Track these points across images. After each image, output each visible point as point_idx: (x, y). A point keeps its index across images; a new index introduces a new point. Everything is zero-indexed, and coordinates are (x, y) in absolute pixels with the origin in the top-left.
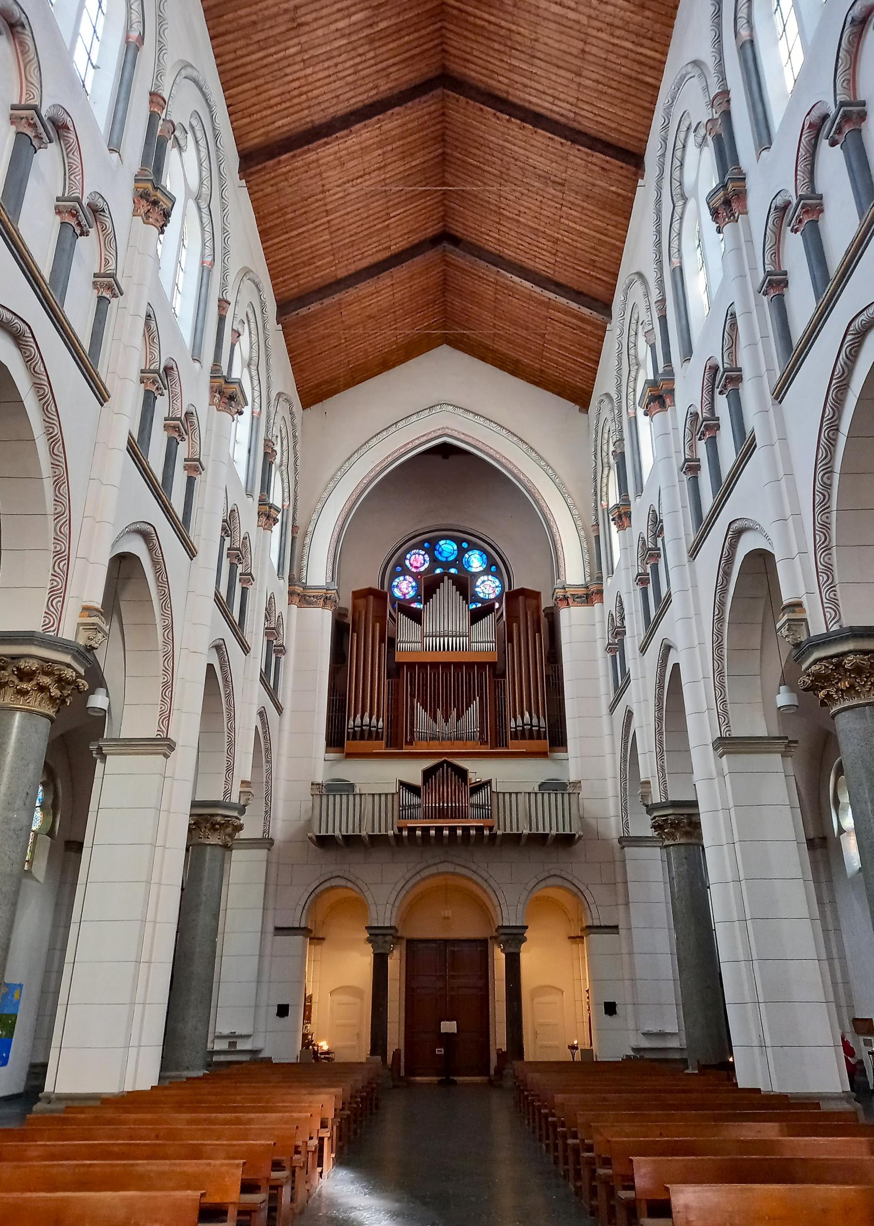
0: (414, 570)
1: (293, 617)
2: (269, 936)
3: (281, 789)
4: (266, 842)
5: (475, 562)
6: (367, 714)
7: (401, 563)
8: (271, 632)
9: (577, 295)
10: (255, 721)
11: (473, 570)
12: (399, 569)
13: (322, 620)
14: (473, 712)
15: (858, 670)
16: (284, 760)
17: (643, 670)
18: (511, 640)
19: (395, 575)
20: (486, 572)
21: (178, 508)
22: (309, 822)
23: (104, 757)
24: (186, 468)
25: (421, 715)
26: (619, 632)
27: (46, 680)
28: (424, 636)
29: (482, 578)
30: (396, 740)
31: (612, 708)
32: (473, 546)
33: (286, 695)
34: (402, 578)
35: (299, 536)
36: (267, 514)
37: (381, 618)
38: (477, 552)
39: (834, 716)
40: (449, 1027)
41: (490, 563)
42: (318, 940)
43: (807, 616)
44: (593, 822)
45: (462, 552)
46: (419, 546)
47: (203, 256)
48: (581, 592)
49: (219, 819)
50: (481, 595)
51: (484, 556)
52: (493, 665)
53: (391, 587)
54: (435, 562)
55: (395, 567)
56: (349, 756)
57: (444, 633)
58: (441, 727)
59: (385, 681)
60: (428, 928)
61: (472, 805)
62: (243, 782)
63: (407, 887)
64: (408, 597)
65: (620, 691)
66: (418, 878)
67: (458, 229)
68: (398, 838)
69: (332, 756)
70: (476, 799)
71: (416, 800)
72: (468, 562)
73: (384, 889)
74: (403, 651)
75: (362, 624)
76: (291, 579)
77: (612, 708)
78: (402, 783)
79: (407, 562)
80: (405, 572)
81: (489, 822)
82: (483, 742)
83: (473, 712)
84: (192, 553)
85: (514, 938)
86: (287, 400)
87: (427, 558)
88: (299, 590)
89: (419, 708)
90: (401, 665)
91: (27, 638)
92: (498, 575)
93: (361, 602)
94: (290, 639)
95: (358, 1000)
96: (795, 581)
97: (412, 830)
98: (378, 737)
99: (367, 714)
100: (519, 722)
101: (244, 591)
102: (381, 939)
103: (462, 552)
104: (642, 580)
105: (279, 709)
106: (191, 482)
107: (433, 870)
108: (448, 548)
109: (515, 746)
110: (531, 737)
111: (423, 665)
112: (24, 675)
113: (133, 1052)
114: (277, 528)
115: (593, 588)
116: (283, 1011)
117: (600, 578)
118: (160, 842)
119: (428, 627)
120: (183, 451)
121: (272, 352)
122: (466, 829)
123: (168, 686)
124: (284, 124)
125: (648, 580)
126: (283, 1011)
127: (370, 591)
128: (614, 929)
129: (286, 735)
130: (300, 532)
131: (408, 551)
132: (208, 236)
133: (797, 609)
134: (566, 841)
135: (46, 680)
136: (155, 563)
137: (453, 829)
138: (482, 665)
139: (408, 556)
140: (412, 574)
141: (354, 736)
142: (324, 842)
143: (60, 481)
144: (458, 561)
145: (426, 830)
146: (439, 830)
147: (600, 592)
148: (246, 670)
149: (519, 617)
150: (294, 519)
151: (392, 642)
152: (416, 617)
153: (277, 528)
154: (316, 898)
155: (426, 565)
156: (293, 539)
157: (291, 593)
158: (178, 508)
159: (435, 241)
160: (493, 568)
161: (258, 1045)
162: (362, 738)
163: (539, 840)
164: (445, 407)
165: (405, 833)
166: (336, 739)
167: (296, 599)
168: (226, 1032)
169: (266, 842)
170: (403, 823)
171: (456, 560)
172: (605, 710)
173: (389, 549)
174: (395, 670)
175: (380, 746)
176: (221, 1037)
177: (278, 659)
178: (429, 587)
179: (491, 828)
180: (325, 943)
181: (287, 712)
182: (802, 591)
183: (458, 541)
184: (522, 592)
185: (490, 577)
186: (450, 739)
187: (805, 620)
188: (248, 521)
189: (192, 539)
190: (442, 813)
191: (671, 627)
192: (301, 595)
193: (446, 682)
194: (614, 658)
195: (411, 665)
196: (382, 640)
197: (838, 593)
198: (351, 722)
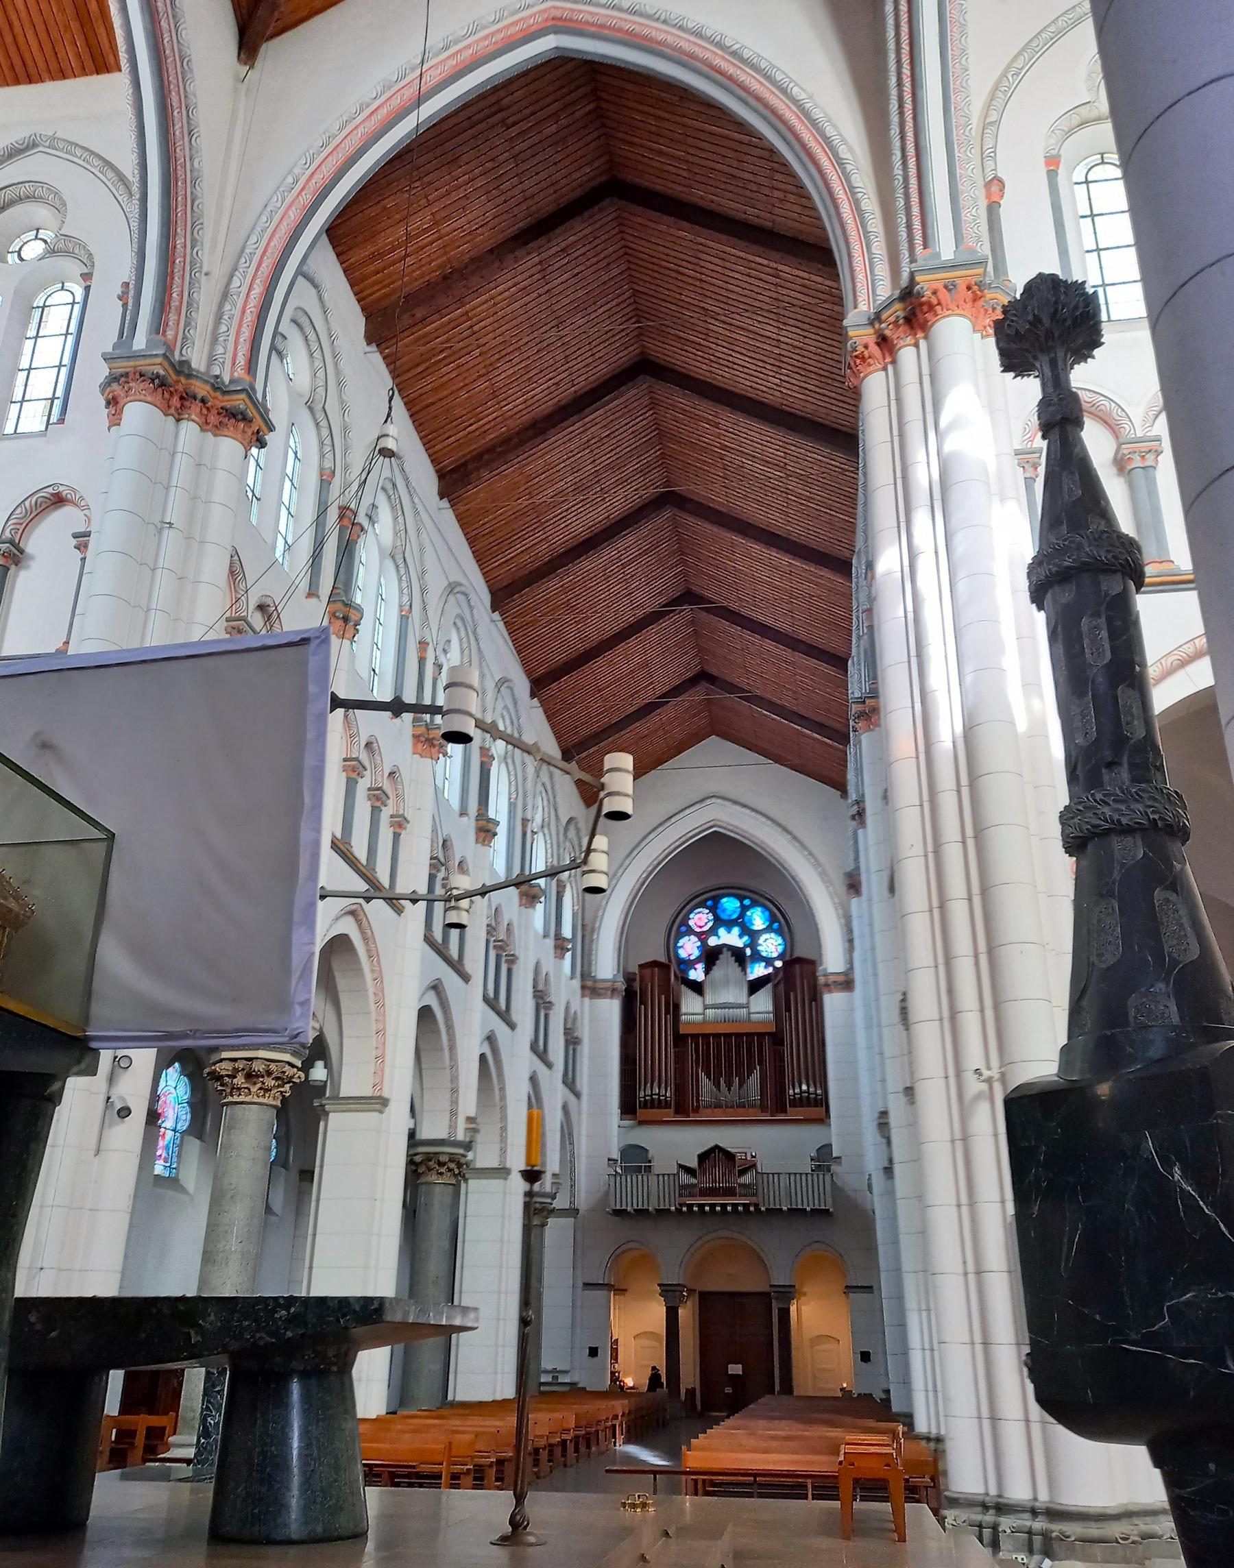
0: (698, 930)
1: (585, 1007)
2: (580, 1290)
3: (582, 1166)
4: (573, 1212)
5: (758, 919)
6: (656, 1084)
7: (685, 922)
9: (820, 727)
10: (559, 1115)
11: (755, 928)
12: (683, 929)
13: (611, 1009)
14: (754, 1080)
16: (584, 1139)
18: (788, 1009)
19: (680, 935)
20: (769, 929)
22: (607, 1194)
23: (466, 1180)
25: (706, 1083)
27: (452, 1165)
28: (706, 1007)
29: (764, 937)
30: (683, 1108)
32: (755, 903)
33: (583, 1084)
34: (687, 938)
35: (587, 933)
36: (561, 946)
37: (666, 988)
38: (759, 909)
40: (735, 1369)
41: (773, 919)
42: (621, 1291)
44: (850, 1193)
45: (744, 909)
46: (702, 905)
47: (510, 794)
48: (841, 978)
50: (764, 954)
51: (767, 913)
52: (769, 1034)
53: (676, 948)
54: (719, 922)
55: (679, 927)
56: (641, 1123)
57: (724, 1002)
58: (725, 1095)
59: (671, 1050)
60: (717, 1283)
61: (740, 1185)
62: (554, 1175)
63: (692, 1250)
64: (692, 958)
66: (700, 1242)
67: (713, 671)
68: (679, 1211)
69: (627, 1123)
70: (746, 1179)
71: (694, 1181)
72: (750, 920)
73: (674, 1253)
74: (689, 1023)
75: (648, 990)
76: (582, 975)
78: (681, 1166)
79: (691, 923)
80: (690, 932)
81: (754, 1200)
82: (763, 1108)
83: (754, 1080)
85: (787, 1293)
87: (711, 917)
88: (589, 983)
89: (702, 1076)
90: (686, 1036)
91: (441, 1142)
92: (779, 932)
93: (648, 971)
94: (584, 1032)
95: (656, 1344)
97: (690, 1206)
98: (667, 1105)
99: (656, 1084)
100: (797, 1091)
101: (546, 1016)
102: (672, 1295)
103: (744, 909)
105: (578, 1095)
107: (713, 1235)
108: (730, 905)
109: (792, 1113)
110: (809, 1105)
111: (706, 1036)
112: (441, 1164)
113: (499, 1377)
114: (568, 955)
116: (593, 1352)
118: (505, 1239)
119: (709, 999)
122: (735, 1206)
123: (504, 1129)
124: (559, 656)
126: (593, 1352)
127: (655, 964)
128: (868, 1289)
129: (584, 1117)
130: (589, 928)
131: (691, 911)
132: (513, 778)
134: (822, 1213)
135: (452, 1165)
137: (724, 1206)
138: (761, 1035)
139: (691, 916)
140: (696, 934)
141: (645, 1105)
142: (619, 1213)
143: (452, 1047)
144: (740, 922)
145: (701, 1206)
146: (713, 1206)
148: (552, 1082)
149: (795, 983)
150: (583, 919)
151: (677, 1007)
152: (697, 988)
153: (568, 955)
154: (616, 1257)
155: (711, 924)
156: (583, 937)
157: (583, 987)
158: (503, 1005)
159: (693, 681)
160: (776, 925)
161: (576, 1379)
162: (653, 1107)
163: (795, 1212)
164: (713, 800)
165: (684, 1209)
166: (629, 1107)
167: (587, 992)
168: (550, 1367)
169: (573, 1212)
170: (683, 1200)
171: (738, 918)
173: (673, 910)
174: (680, 1039)
175: (669, 1114)
176: (546, 1372)
178: (711, 957)
179: (756, 1205)
180: (627, 1294)
181: (585, 1097)
183: (741, 898)
184: (800, 960)
185: (773, 935)
186: (732, 1107)
188: (548, 965)
190: (712, 1192)
192: (591, 988)
193: (729, 1051)
195: (695, 1037)
196: (667, 1012)
198: (642, 1094)
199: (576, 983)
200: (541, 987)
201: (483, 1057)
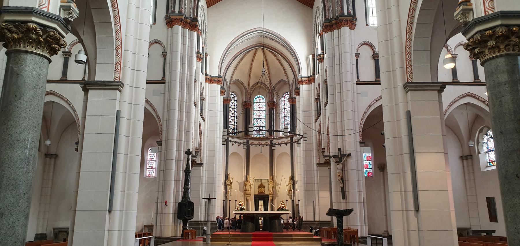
49: (32, 25)
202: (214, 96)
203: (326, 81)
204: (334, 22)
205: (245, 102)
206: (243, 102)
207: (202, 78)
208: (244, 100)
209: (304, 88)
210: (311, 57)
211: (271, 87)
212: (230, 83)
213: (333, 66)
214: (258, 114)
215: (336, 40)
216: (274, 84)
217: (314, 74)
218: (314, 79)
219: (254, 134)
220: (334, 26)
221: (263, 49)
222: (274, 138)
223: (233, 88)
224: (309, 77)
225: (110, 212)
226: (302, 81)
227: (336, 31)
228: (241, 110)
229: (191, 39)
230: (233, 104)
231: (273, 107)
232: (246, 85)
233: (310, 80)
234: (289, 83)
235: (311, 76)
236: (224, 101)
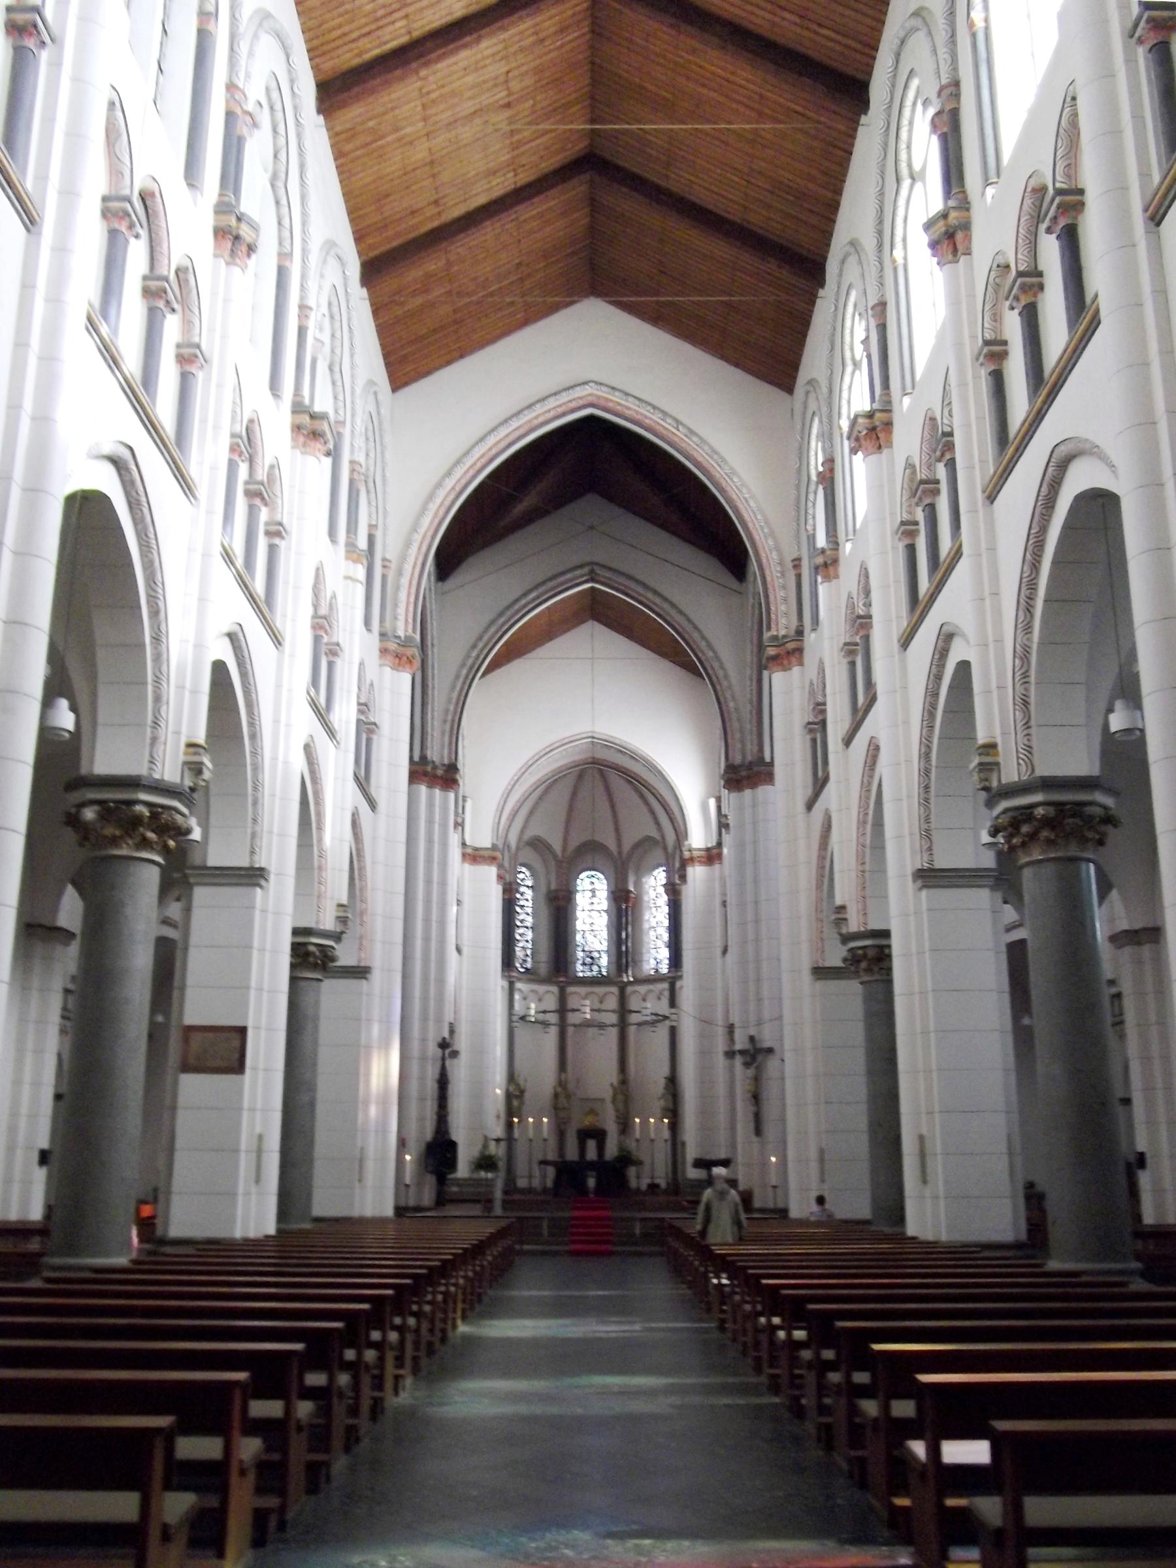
8: (364, 707)
15: (1047, 822)
17: (846, 767)
21: (259, 586)
24: (268, 533)
26: (820, 708)
31: (810, 806)
39: (1022, 867)
43: (1000, 759)
65: (820, 783)
76: (383, 635)
77: (810, 806)
84: (277, 640)
86: (375, 393)
96: (992, 718)
104: (849, 649)
106: (272, 550)
115: (791, 646)
117: (800, 632)
120: (264, 515)
121: (357, 342)
125: (858, 649)
130: (393, 566)
133: (991, 751)
136: (241, 664)
147: (800, 651)
167: (389, 659)
172: (800, 807)
177: (369, 741)
182: (998, 731)
187: (997, 764)
189: (278, 625)
191: (877, 723)
194: (814, 741)
197: (1034, 738)
199: (374, 640)
200: (323, 611)
201: (219, 668)
202: (485, 885)
203: (724, 904)
204: (744, 773)
205: (556, 891)
206: (549, 892)
207: (455, 853)
208: (553, 887)
209: (697, 873)
210: (712, 803)
211: (620, 853)
212: (518, 848)
213: (740, 865)
214: (589, 921)
215: (748, 812)
216: (626, 847)
217: (719, 844)
218: (719, 856)
219: (581, 971)
220: (745, 782)
221: (601, 772)
222: (630, 983)
223: (528, 854)
224: (708, 850)
225: (360, 1181)
226: (692, 859)
227: (748, 792)
228: (545, 913)
229: (445, 809)
230: (527, 898)
231: (624, 909)
232: (557, 847)
233: (712, 856)
234: (665, 848)
235: (713, 848)
236: (505, 891)
